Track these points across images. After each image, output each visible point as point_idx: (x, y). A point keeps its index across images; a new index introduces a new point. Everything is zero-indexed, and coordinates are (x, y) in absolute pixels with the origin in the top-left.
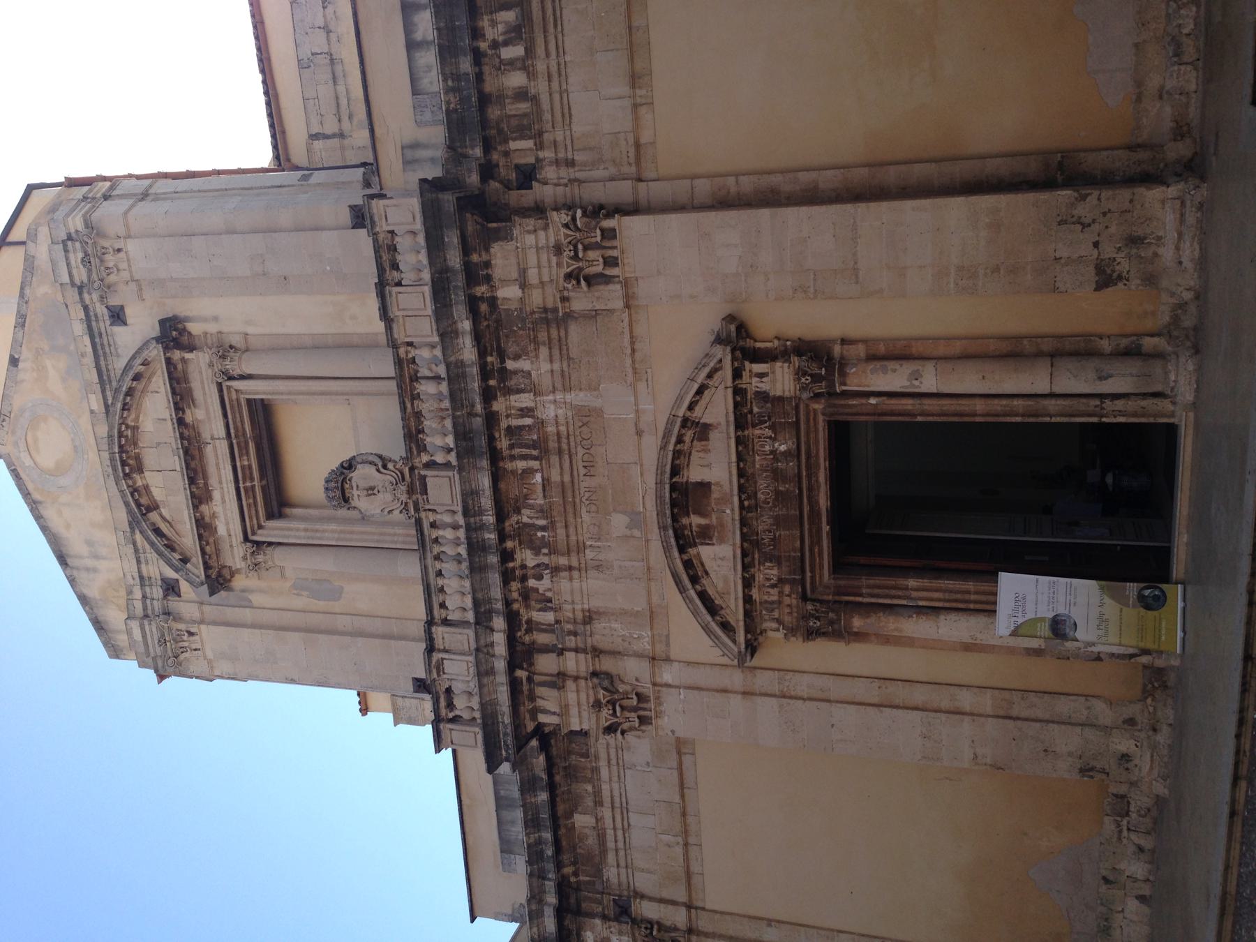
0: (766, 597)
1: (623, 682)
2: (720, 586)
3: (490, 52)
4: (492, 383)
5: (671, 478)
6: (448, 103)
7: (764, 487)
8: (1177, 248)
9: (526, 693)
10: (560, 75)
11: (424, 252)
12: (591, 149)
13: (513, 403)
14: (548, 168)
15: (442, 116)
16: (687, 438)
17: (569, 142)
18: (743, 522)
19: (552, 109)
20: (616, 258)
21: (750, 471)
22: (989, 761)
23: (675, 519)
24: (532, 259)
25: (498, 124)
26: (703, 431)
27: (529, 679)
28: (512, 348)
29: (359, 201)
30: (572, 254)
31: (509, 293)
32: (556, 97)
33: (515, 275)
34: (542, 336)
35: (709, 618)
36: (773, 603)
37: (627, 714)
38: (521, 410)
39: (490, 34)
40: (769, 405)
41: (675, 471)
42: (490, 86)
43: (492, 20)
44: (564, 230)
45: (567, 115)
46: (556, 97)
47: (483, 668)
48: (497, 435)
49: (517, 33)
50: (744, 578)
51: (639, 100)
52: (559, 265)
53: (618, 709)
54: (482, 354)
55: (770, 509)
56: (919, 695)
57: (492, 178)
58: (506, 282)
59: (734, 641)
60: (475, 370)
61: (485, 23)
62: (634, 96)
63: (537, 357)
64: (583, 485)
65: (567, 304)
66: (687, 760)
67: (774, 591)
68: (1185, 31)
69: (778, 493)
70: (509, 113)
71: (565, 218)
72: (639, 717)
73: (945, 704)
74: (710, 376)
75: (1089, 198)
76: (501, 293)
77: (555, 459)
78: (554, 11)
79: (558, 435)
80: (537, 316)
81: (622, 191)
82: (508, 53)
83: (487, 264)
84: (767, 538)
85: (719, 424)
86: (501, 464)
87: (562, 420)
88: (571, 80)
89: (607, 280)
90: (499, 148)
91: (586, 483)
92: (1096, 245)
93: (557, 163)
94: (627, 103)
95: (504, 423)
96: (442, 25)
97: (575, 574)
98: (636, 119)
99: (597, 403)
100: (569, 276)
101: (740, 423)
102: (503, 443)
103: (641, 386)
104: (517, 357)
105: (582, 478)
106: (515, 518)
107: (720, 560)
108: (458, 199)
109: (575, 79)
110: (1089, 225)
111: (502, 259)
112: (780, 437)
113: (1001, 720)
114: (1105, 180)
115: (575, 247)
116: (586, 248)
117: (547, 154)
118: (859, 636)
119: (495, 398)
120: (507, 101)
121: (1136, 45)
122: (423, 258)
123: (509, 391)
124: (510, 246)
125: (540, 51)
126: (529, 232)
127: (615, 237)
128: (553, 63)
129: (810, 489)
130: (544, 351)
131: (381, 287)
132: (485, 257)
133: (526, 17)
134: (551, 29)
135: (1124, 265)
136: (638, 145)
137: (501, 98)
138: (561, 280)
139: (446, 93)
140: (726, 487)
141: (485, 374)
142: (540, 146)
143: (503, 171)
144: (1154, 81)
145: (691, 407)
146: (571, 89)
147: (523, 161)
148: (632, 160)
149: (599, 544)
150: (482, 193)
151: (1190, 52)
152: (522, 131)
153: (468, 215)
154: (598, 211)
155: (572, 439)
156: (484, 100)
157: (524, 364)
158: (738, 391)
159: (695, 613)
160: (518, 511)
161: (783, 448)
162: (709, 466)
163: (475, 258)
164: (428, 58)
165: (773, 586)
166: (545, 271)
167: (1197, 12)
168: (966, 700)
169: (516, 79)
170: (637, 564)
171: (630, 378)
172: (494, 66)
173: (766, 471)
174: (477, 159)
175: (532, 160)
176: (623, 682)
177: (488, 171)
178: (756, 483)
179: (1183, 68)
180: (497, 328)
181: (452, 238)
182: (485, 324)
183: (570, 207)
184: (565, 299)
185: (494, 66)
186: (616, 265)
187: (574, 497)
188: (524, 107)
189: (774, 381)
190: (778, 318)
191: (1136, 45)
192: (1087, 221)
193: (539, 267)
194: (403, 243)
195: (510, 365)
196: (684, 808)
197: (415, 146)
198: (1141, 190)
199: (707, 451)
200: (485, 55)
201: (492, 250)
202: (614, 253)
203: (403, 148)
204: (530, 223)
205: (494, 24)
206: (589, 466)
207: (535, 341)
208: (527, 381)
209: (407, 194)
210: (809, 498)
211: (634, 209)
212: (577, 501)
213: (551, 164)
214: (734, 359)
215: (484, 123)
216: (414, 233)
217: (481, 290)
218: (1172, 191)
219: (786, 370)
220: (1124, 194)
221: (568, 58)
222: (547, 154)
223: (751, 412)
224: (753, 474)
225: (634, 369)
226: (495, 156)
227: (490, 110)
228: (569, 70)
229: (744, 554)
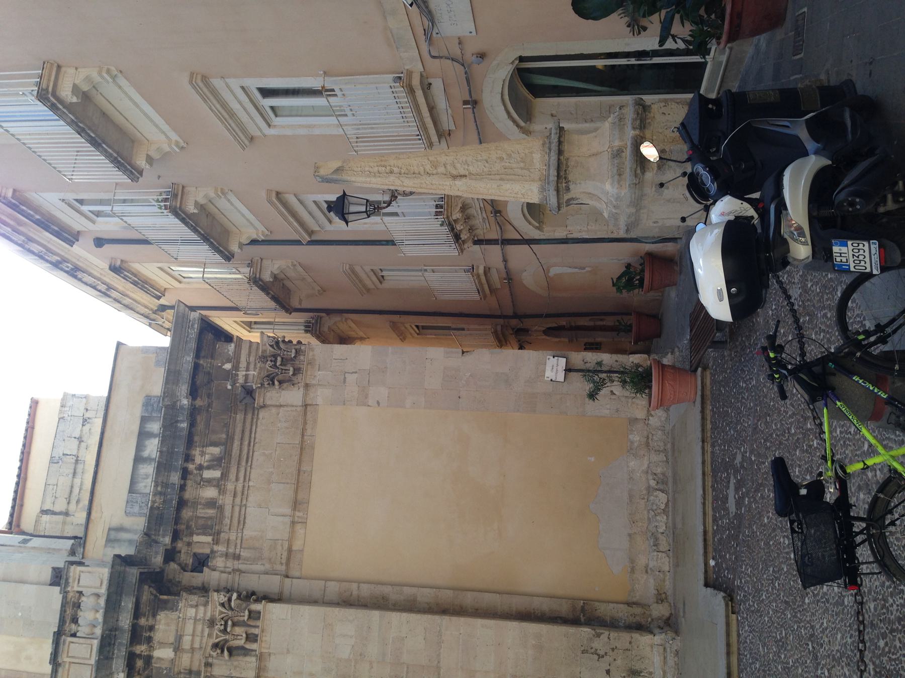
3: (195, 472)
6: (154, 502)
10: (243, 494)
11: (102, 611)
12: (254, 549)
15: (146, 511)
17: (239, 542)
20: (257, 636)
25: (188, 522)
29: (61, 565)
30: (222, 627)
31: (163, 654)
32: (237, 509)
33: (172, 639)
39: (198, 460)
42: (187, 495)
43: (203, 452)
44: (220, 608)
45: (242, 522)
46: (237, 509)
49: (217, 462)
51: (296, 519)
52: (210, 635)
57: (173, 560)
58: (162, 644)
61: (196, 452)
65: (209, 669)
68: (661, 530)
70: (198, 515)
71: (223, 598)
76: (157, 653)
78: (249, 450)
81: (271, 584)
82: (207, 474)
83: (151, 628)
88: (250, 499)
89: (245, 652)
90: (184, 539)
93: (227, 555)
94: (288, 520)
96: (164, 449)
98: (293, 532)
100: (216, 646)
108: (141, 573)
109: (254, 498)
110: (603, 657)
111: (164, 625)
114: (612, 624)
115: (226, 625)
116: (234, 625)
120: (199, 507)
121: (630, 535)
122: (100, 616)
124: (174, 615)
125: (232, 476)
126: (192, 606)
127: (259, 618)
131: (58, 636)
132: (151, 622)
133: (227, 453)
134: (244, 463)
136: (290, 550)
137: (195, 504)
138: (209, 648)
139: (155, 495)
142: (216, 542)
144: (642, 561)
146: (248, 505)
147: (201, 551)
148: (284, 561)
150: (162, 571)
151: (664, 546)
152: (205, 529)
153: (146, 587)
154: (250, 596)
156: (182, 503)
163: (142, 621)
164: (148, 470)
166: (198, 639)
167: (667, 519)
169: (210, 493)
174: (165, 545)
175: (208, 551)
177: (171, 555)
179: (660, 554)
181: (128, 604)
183: (228, 591)
184: (208, 665)
185: (195, 482)
186: (256, 641)
188: (211, 512)
191: (630, 535)
192: (601, 653)
193: (193, 636)
194: (87, 602)
197: (120, 529)
198: (636, 635)
200: (191, 473)
201: (158, 617)
202: (256, 631)
203: (110, 529)
204: (194, 599)
205: (203, 454)
209: (102, 564)
211: (278, 599)
215: (177, 520)
216: (98, 596)
218: (658, 639)
220: (625, 636)
221: (251, 484)
222: (221, 548)
226: (180, 545)
227: (184, 511)
228: (250, 492)
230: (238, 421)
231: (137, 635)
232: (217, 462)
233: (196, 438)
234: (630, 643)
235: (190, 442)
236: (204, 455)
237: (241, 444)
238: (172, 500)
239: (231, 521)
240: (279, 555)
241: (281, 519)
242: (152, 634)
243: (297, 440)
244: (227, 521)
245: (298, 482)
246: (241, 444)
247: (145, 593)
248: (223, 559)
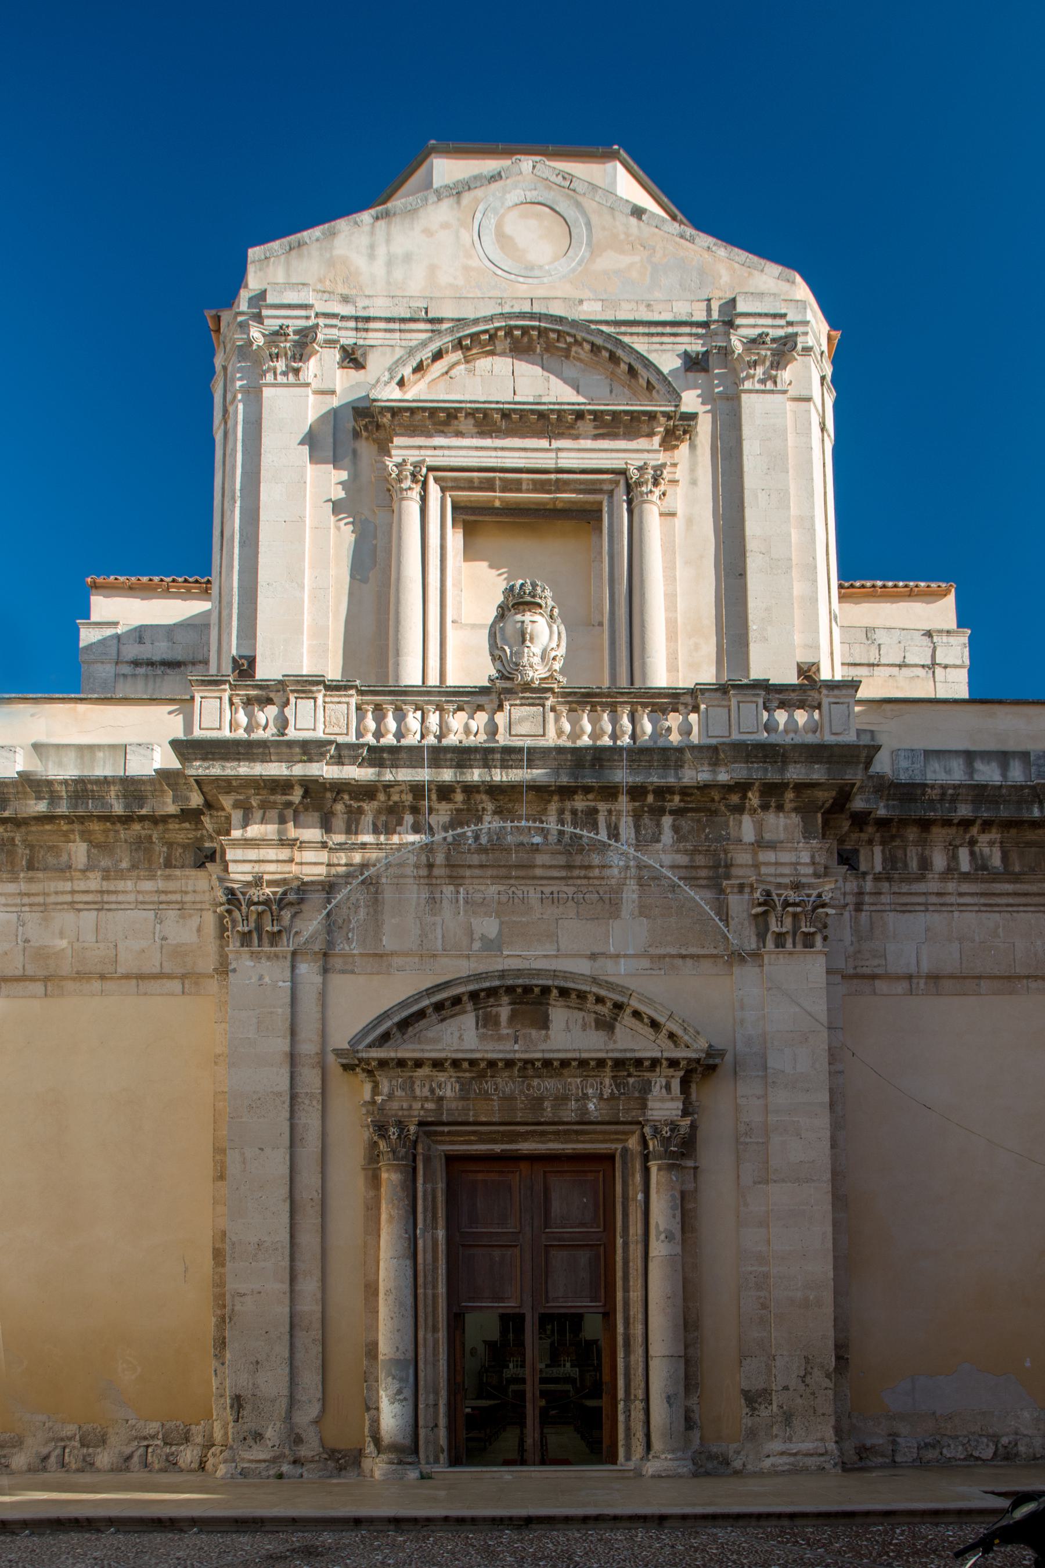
0: (418, 1083)
1: (294, 916)
2: (430, 1034)
3: (968, 836)
4: (650, 798)
5: (557, 987)
7: (549, 1085)
8: (782, 1453)
9: (272, 798)
13: (624, 819)
14: (855, 883)
16: (599, 1008)
17: (879, 908)
18: (509, 1063)
19: (911, 894)
20: (783, 947)
21: (565, 1072)
22: (238, 1308)
23: (510, 990)
24: (786, 857)
26: (606, 1025)
27: (289, 804)
28: (685, 824)
31: (747, 828)
32: (921, 899)
34: (700, 860)
35: (396, 1019)
36: (413, 1090)
37: (253, 918)
38: (616, 828)
39: (984, 838)
40: (637, 1094)
41: (564, 992)
42: (939, 834)
43: (994, 843)
45: (905, 909)
46: (921, 899)
47: (345, 752)
48: (590, 796)
49: (981, 866)
50: (446, 1060)
51: (915, 981)
52: (779, 886)
53: (260, 908)
54: (685, 792)
55: (522, 1092)
56: (309, 1239)
58: (759, 827)
59: (370, 1046)
60: (671, 780)
61: (994, 835)
62: (919, 977)
63: (678, 851)
64: (531, 889)
65: (736, 890)
66: (176, 985)
67: (426, 1092)
69: (541, 1099)
70: (909, 849)
72: (250, 932)
73: (301, 1266)
74: (672, 1036)
75: (827, 1380)
76: (747, 821)
77: (561, 860)
79: (589, 867)
80: (722, 856)
82: (964, 854)
83: (780, 808)
84: (488, 1086)
85: (615, 1042)
86: (556, 798)
87: (607, 872)
88: (936, 915)
90: (878, 835)
91: (533, 895)
92: (786, 1388)
93: (861, 894)
94: (913, 969)
95: (602, 807)
97: (424, 872)
98: (898, 978)
99: (625, 913)
101: (619, 1064)
102: (580, 803)
103: (645, 963)
104: (676, 829)
105: (539, 889)
106: (490, 807)
107: (461, 1036)
109: (937, 920)
110: (803, 1382)
112: (603, 1104)
113: (288, 1320)
116: (795, 915)
117: (869, 885)
118: (374, 1181)
119: (633, 799)
120: (920, 848)
123: (637, 816)
124: (798, 835)
125: (965, 888)
126: (813, 857)
127: (805, 946)
128: (952, 899)
129: (543, 1133)
130: (683, 860)
132: (788, 806)
133: (995, 877)
134: (983, 901)
135: (764, 1412)
136: (874, 977)
137: (923, 843)
138: (764, 887)
140: (543, 1047)
141: (662, 792)
142: (877, 878)
143: (854, 836)
145: (637, 1014)
147: (862, 858)
148: (859, 970)
149: (461, 901)
152: (891, 861)
155: (584, 882)
156: (925, 825)
157: (667, 836)
158: (655, 1062)
159: (403, 1005)
160: (498, 812)
161: (591, 1106)
162: (568, 1029)
165: (432, 1091)
166: (771, 870)
168: (309, 1286)
169: (939, 861)
170: (440, 941)
171: (653, 951)
172: (954, 839)
173: (564, 1089)
175: (863, 868)
176: (294, 916)
178: (551, 1077)
180: (709, 810)
182: (717, 798)
185: (954, 839)
186: (777, 947)
187: (517, 878)
188: (914, 865)
189: (662, 1100)
190: (723, 1106)
192: (808, 1380)
193: (776, 864)
195: (667, 821)
196: (111, 978)
199: (584, 1027)
200: (966, 831)
201: (793, 815)
205: (991, 844)
206: (554, 900)
207: (695, 851)
208: (649, 837)
210: (535, 1131)
212: (512, 882)
213: (860, 887)
214: (690, 1060)
215: (903, 823)
217: (754, 798)
219: (674, 1112)
221: (956, 914)
222: (869, 885)
223: (630, 1075)
224: (561, 1075)
225: (664, 956)
226: (870, 829)
227: (915, 829)
228: (945, 914)
229: (473, 1062)
230: (1039, 885)
231: (772, 792)
232: (981, 866)
233: (1013, 831)
234: (823, 1415)
235: (1008, 825)
236: (990, 848)
237: (1008, 894)
238: (934, 810)
239: (904, 894)
240: (867, 963)
241: (913, 961)
242: (772, 810)
243: (1020, 970)
244: (905, 888)
245: (965, 978)
246: (1008, 894)
247: (826, 794)
248: (856, 890)
